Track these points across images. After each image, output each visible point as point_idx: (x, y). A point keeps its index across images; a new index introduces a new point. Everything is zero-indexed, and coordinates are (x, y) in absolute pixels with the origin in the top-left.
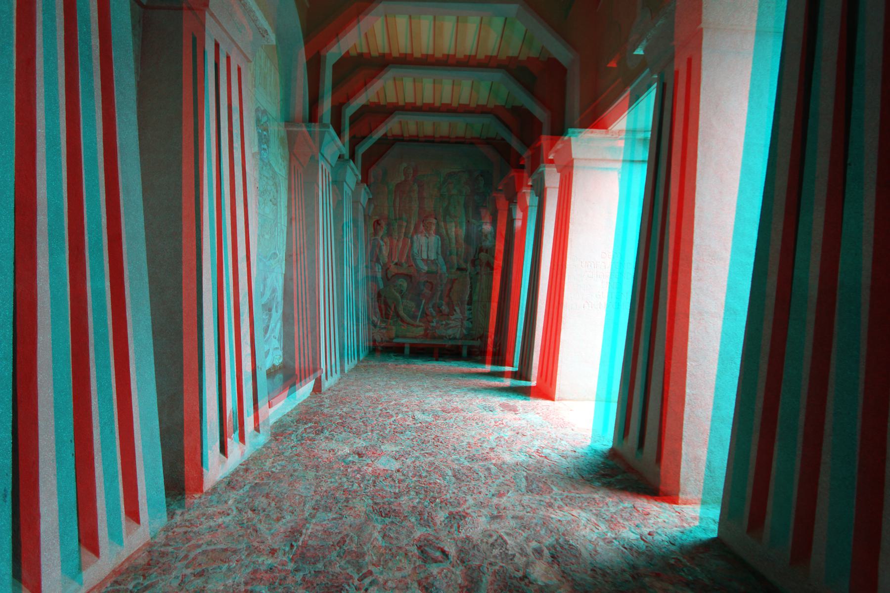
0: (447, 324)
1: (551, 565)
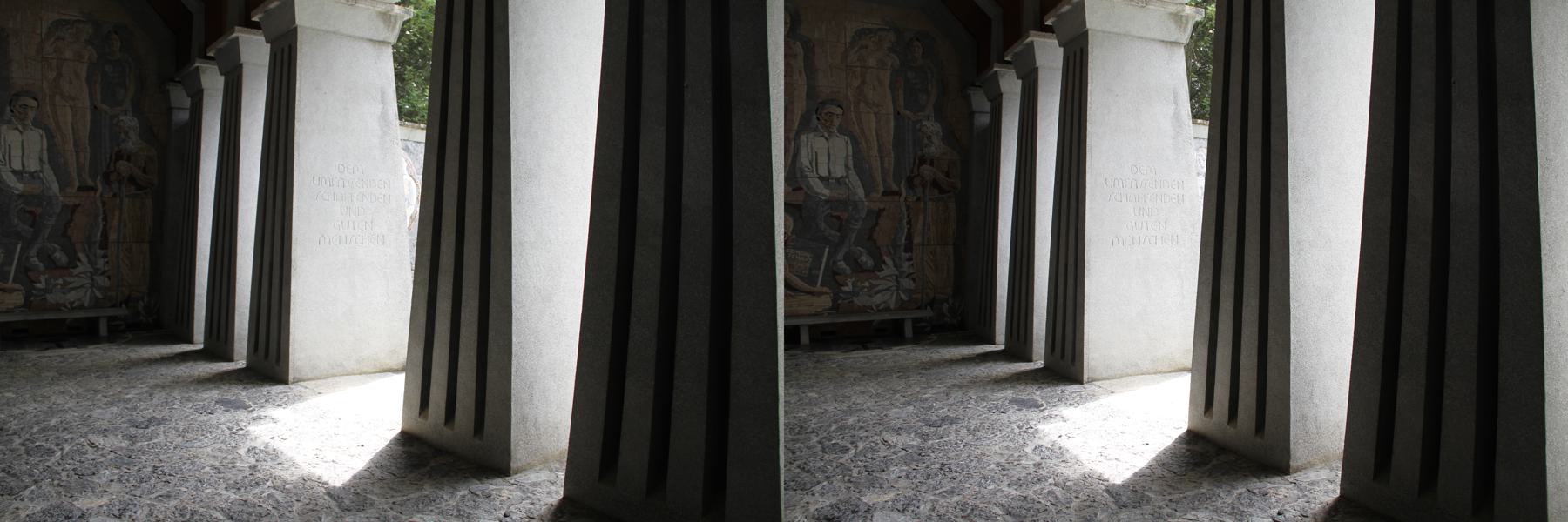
0: (872, 286)
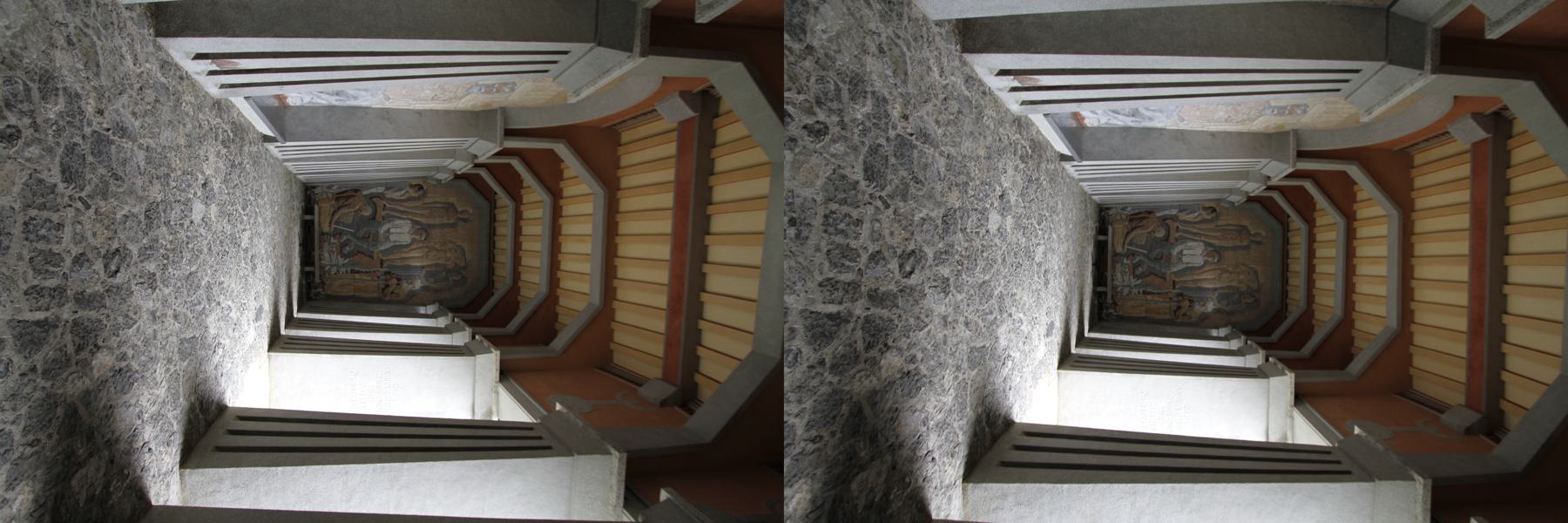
1: (112, 369)
